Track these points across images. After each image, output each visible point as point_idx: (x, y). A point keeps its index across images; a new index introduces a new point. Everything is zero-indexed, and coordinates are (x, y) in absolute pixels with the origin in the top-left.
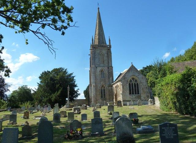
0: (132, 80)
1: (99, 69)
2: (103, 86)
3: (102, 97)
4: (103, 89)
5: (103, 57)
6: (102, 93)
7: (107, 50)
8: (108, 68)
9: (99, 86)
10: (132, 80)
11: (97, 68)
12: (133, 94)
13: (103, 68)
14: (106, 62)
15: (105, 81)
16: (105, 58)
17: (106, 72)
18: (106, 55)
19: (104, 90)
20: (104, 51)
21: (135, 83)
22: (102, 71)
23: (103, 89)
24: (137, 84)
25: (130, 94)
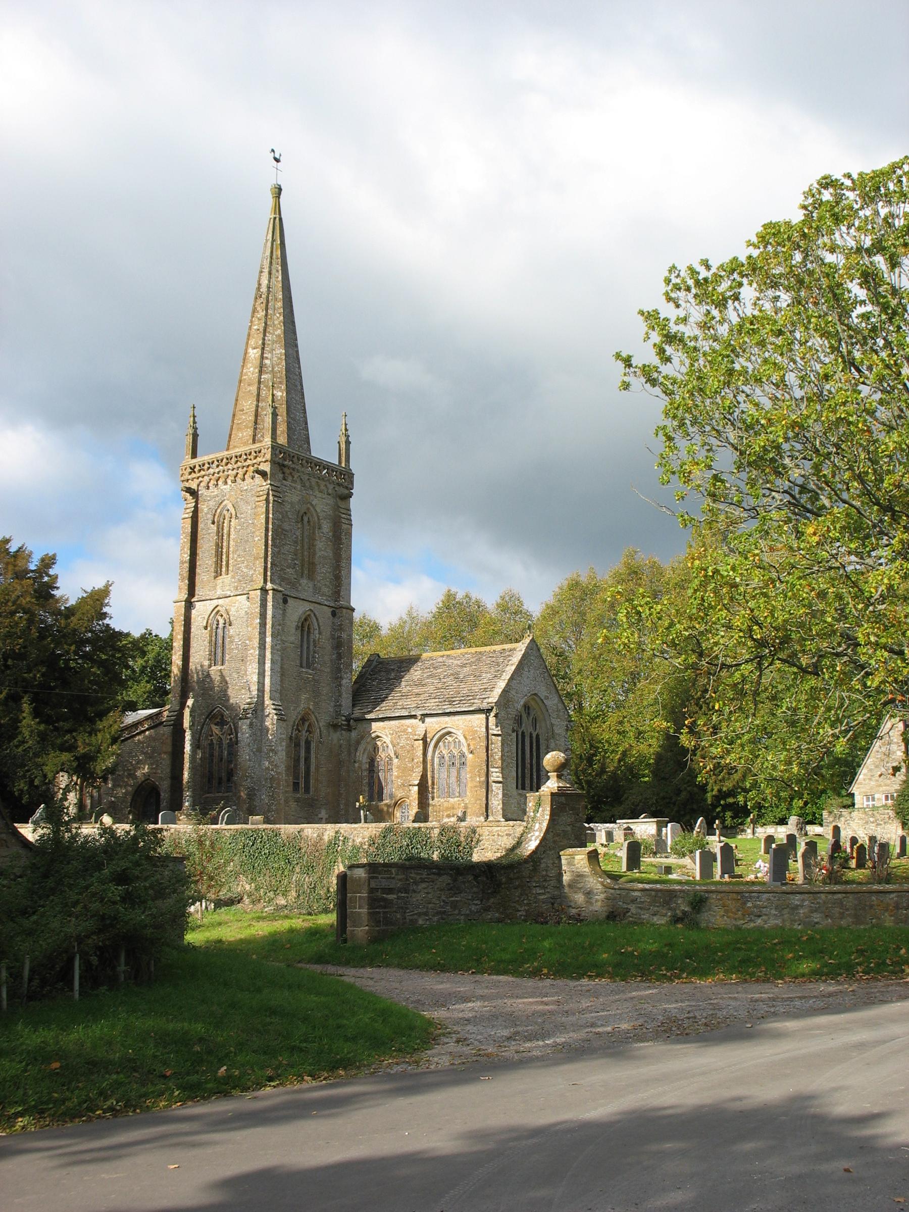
0: (524, 716)
1: (297, 610)
2: (303, 720)
3: (296, 785)
4: (303, 739)
5: (312, 539)
6: (297, 761)
7: (331, 501)
8: (334, 614)
9: (294, 716)
10: (524, 716)
11: (285, 601)
12: (523, 788)
13: (312, 606)
14: (324, 571)
15: (316, 694)
16: (323, 548)
17: (323, 636)
18: (326, 527)
19: (308, 743)
20: (322, 504)
21: (531, 734)
22: (304, 626)
23: (303, 739)
24: (538, 736)
25: (517, 788)
